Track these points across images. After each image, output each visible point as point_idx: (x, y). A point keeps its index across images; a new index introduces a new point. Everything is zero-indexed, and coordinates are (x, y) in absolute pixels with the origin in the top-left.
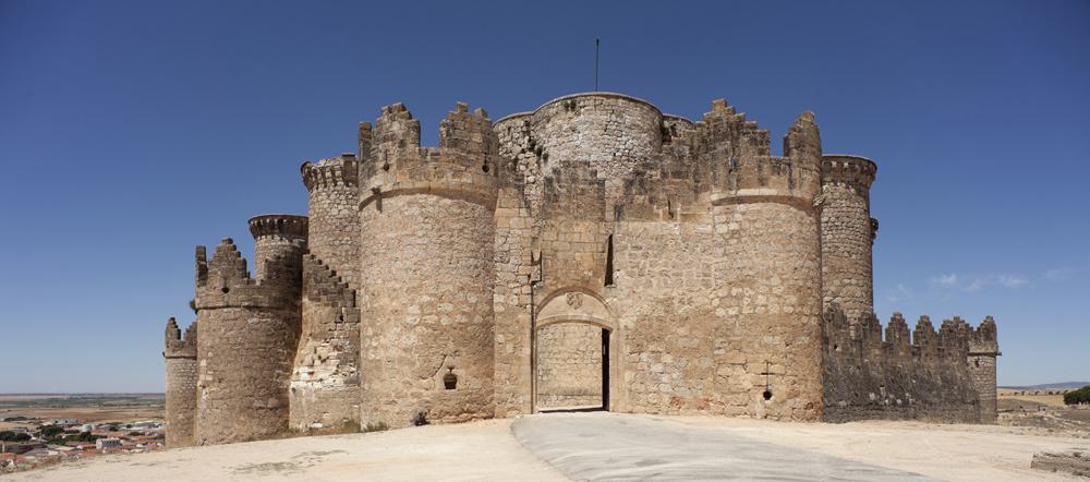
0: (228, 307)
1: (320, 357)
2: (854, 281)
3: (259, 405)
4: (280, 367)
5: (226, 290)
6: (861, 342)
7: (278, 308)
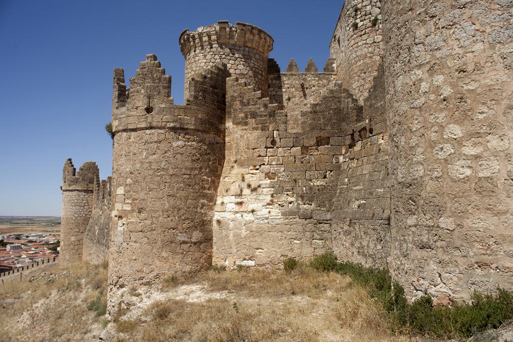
0: (151, 128)
1: (249, 186)
3: (183, 239)
4: (204, 196)
5: (149, 110)
7: (204, 131)
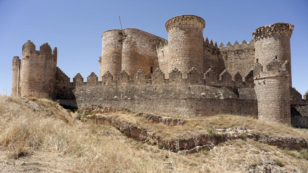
2: (178, 59)
6: (117, 81)
